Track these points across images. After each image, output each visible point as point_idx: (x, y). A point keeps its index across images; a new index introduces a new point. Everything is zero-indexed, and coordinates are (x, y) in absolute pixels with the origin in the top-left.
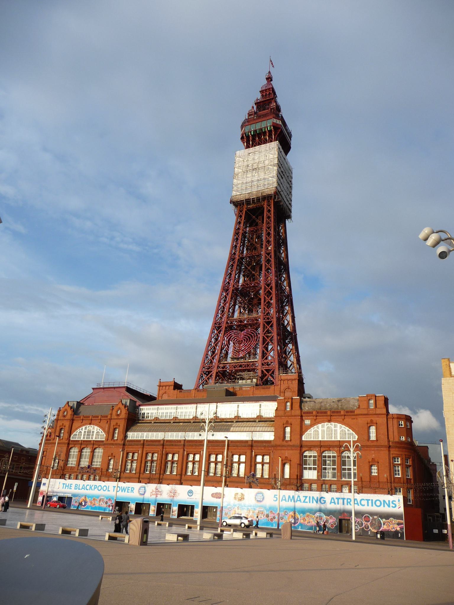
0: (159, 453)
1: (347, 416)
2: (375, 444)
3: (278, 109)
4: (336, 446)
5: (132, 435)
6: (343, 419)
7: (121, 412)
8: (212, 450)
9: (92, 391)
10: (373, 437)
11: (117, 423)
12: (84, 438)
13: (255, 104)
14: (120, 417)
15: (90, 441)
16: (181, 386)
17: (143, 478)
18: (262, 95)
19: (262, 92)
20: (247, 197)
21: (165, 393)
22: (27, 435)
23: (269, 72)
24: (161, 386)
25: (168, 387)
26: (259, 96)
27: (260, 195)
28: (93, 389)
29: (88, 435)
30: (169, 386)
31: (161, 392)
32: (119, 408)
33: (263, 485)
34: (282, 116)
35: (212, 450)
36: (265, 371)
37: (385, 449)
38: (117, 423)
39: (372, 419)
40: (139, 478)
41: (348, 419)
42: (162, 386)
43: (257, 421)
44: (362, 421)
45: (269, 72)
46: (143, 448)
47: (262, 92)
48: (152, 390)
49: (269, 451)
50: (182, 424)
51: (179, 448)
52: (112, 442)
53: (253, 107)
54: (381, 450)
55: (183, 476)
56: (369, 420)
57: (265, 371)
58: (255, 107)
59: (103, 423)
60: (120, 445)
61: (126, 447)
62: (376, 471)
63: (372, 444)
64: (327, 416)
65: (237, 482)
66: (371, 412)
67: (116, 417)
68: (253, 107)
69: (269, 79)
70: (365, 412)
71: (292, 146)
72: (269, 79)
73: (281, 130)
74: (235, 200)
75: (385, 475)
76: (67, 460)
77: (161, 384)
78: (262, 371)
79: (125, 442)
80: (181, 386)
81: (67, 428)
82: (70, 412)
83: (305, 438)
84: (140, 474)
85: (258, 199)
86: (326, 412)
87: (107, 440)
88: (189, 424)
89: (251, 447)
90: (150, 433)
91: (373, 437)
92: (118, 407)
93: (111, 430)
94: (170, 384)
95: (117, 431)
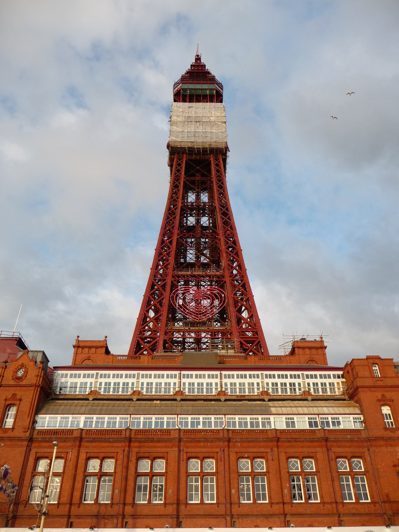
0: (120, 456)
5: (47, 421)
7: (26, 372)
8: (243, 450)
11: (14, 395)
14: (24, 382)
17: (79, 517)
20: (190, 145)
25: (93, 350)
27: (207, 146)
30: (97, 347)
32: (22, 366)
33: (366, 518)
35: (243, 450)
38: (14, 395)
40: (69, 517)
42: (83, 347)
43: (310, 398)
46: (80, 446)
49: (361, 450)
50: (158, 402)
55: (182, 507)
60: (20, 439)
61: (34, 445)
65: (311, 515)
67: (12, 383)
74: (173, 145)
77: (81, 344)
79: (31, 434)
84: (71, 504)
85: (205, 150)
88: (173, 402)
89: (324, 442)
90: (95, 417)
92: (20, 362)
94: (99, 344)
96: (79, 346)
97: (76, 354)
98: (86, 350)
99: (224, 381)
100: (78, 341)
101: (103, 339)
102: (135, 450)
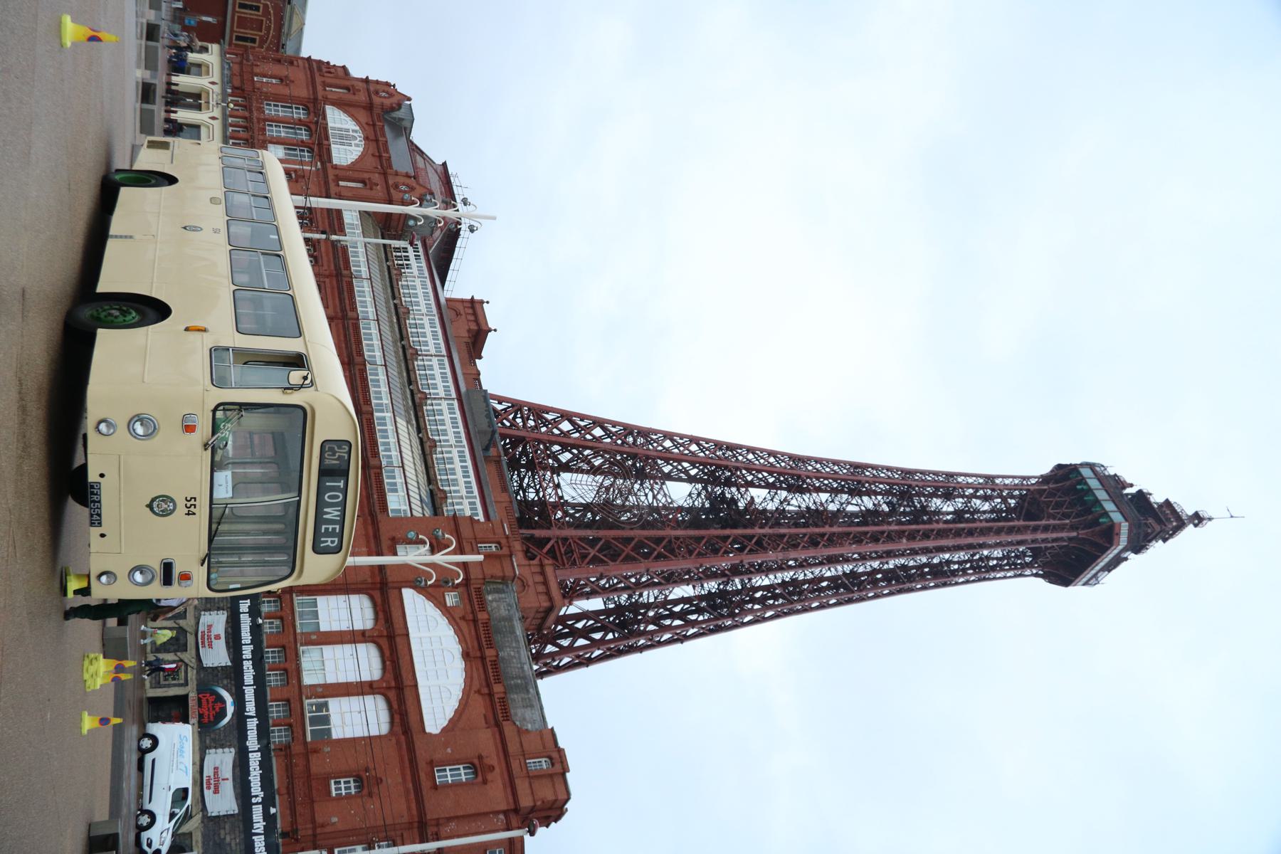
1: (492, 701)
2: (425, 784)
4: (398, 677)
6: (479, 692)
9: (439, 161)
10: (447, 775)
12: (333, 129)
13: (1140, 492)
15: (327, 138)
16: (480, 358)
18: (1161, 506)
19: (1167, 503)
21: (458, 314)
22: (321, 37)
23: (1210, 519)
24: (474, 307)
26: (1157, 498)
28: (444, 164)
29: (341, 137)
30: (476, 321)
31: (460, 307)
34: (1126, 559)
36: (549, 546)
37: (415, 812)
39: (497, 770)
41: (479, 706)
42: (473, 308)
44: (485, 741)
45: (1210, 519)
47: (1167, 503)
48: (459, 285)
51: (335, 307)
52: (331, 177)
53: (1131, 485)
54: (408, 801)
56: (493, 759)
57: (549, 546)
59: (371, 162)
62: (343, 792)
63: (423, 776)
64: (480, 648)
66: (515, 765)
68: (1131, 485)
69: (1198, 519)
70: (513, 747)
71: (1070, 588)
72: (1198, 519)
73: (1107, 549)
75: (335, 820)
76: (278, 98)
77: (477, 306)
78: (549, 539)
80: (480, 358)
81: (350, 97)
82: (387, 102)
83: (408, 593)
86: (491, 646)
87: (335, 167)
91: (447, 775)
93: (356, 175)
95: (360, 185)
96: (474, 307)
97: (462, 301)
98: (470, 311)
99: (444, 404)
100: (482, 302)
101: (491, 325)
102: (327, 280)
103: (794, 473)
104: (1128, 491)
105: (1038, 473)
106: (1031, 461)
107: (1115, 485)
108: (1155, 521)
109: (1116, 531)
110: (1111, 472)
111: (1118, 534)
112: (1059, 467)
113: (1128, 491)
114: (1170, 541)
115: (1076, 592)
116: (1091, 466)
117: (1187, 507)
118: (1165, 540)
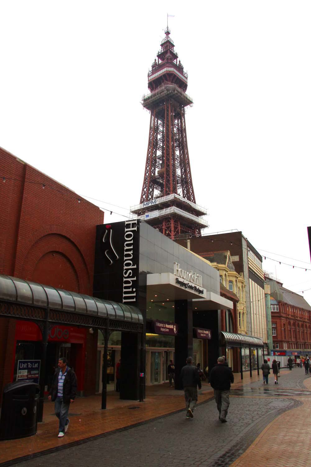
3: (175, 57)
19: (162, 45)
23: (168, 27)
26: (159, 49)
34: (180, 61)
45: (168, 27)
47: (162, 45)
53: (155, 60)
58: (157, 58)
68: (155, 60)
69: (168, 33)
71: (188, 84)
72: (168, 33)
103: (151, 161)
104: (157, 61)
105: (150, 115)
106: (145, 117)
107: (156, 67)
108: (167, 53)
109: (168, 72)
110: (151, 69)
111: (170, 71)
112: (149, 87)
113: (157, 61)
114: (174, 44)
115: (190, 83)
116: (149, 76)
117: (162, 38)
118: (173, 46)
